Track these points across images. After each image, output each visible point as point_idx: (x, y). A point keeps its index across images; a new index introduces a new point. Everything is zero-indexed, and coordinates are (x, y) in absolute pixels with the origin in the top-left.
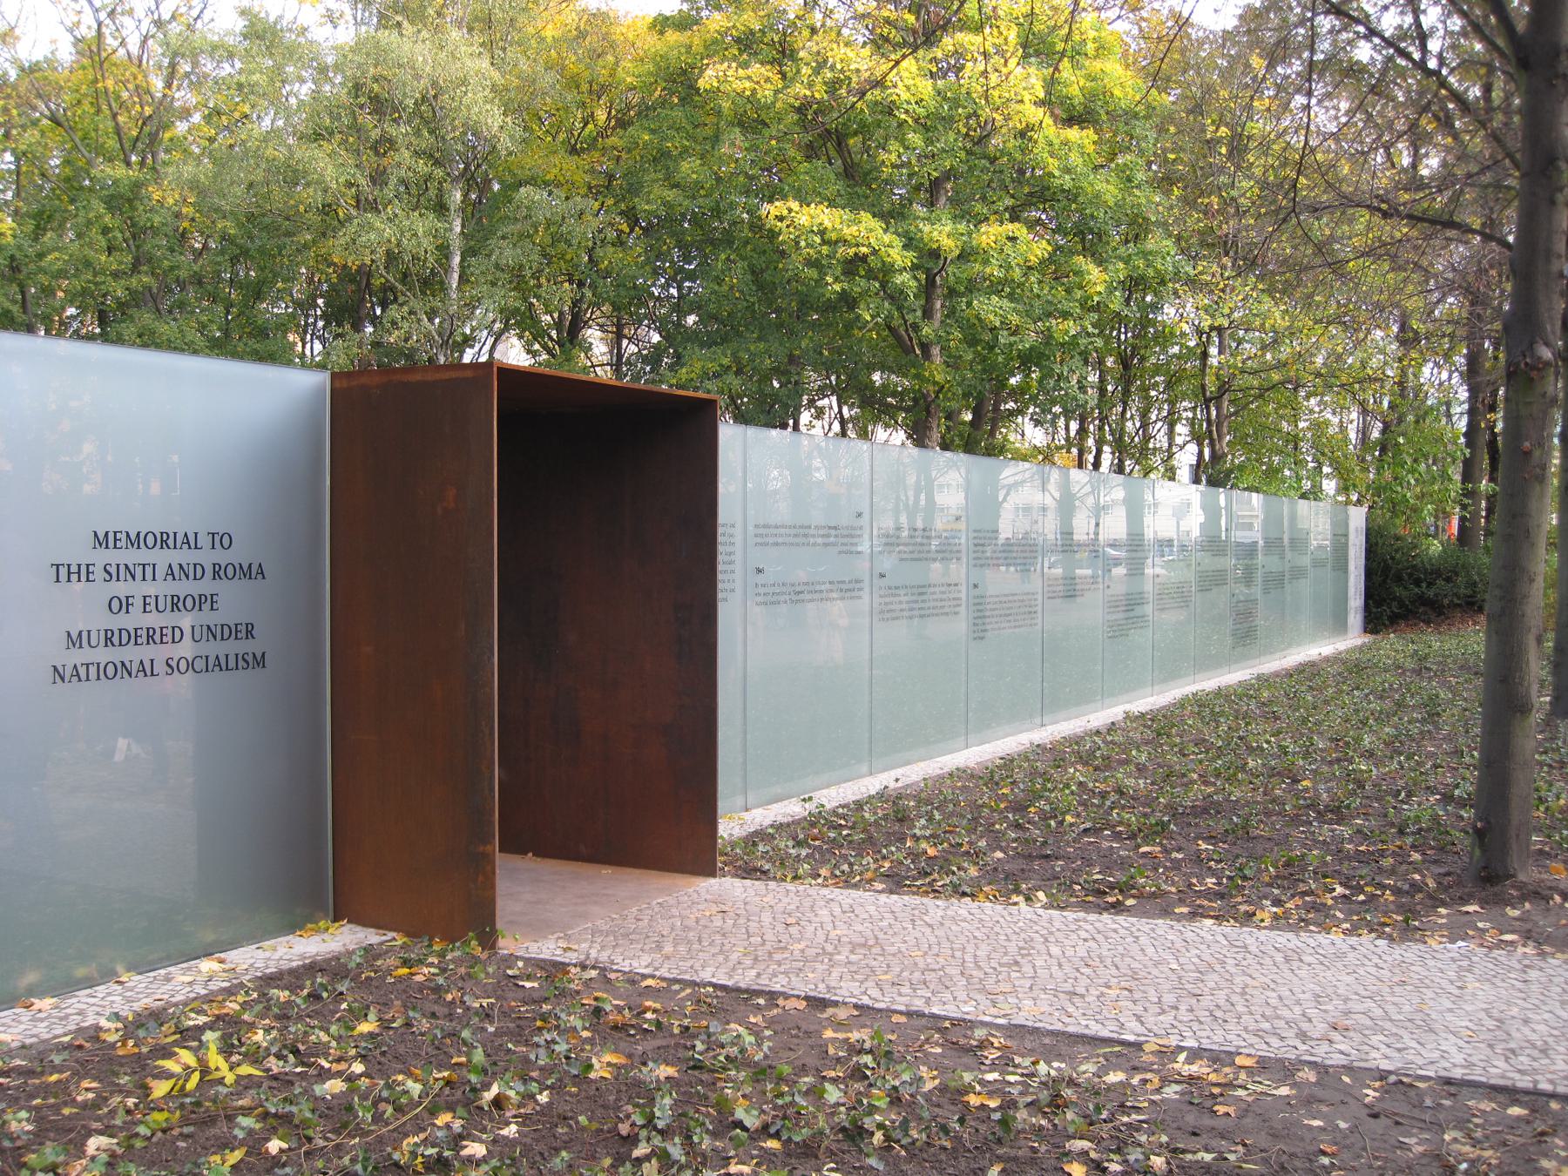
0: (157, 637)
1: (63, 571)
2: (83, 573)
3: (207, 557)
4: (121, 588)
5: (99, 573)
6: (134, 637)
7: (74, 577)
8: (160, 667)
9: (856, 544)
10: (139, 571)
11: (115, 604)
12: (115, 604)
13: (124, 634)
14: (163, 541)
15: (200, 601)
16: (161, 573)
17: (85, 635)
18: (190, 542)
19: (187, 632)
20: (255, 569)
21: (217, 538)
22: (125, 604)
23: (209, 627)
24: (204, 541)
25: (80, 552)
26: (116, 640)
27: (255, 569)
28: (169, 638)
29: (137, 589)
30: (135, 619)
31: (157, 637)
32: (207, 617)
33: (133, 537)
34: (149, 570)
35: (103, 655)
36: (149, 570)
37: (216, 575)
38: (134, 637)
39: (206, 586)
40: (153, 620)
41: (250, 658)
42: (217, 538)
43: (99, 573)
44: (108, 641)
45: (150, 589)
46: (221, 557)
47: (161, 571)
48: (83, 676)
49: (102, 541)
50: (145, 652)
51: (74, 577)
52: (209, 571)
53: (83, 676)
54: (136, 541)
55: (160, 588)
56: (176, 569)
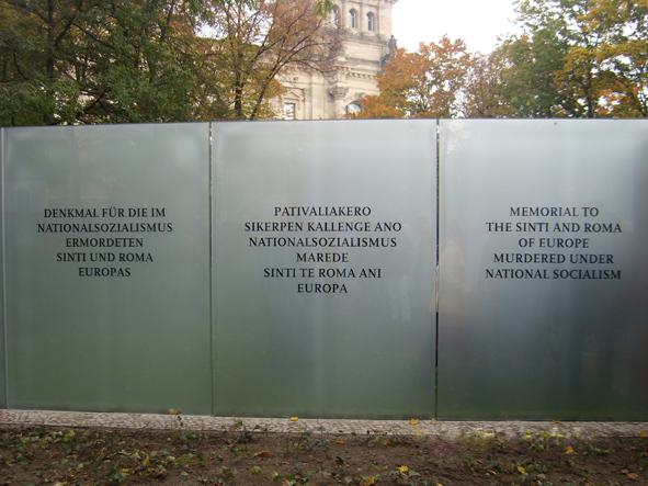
0: (548, 259)
1: (493, 226)
3: (581, 220)
4: (527, 235)
5: (514, 227)
7: (499, 229)
8: (550, 274)
10: (538, 227)
11: (523, 243)
12: (523, 243)
13: (528, 257)
15: (576, 243)
16: (551, 227)
17: (505, 257)
18: (571, 212)
20: (614, 226)
21: (588, 211)
22: (530, 242)
23: (582, 256)
24: (580, 212)
25: (506, 218)
26: (523, 259)
27: (614, 226)
28: (556, 260)
29: (536, 235)
30: (535, 249)
31: (548, 259)
32: (580, 250)
33: (534, 210)
34: (544, 227)
35: (515, 266)
36: (544, 227)
37: (587, 228)
39: (581, 234)
40: (547, 251)
41: (610, 273)
42: (588, 211)
43: (514, 227)
45: (544, 234)
46: (592, 221)
47: (551, 227)
48: (503, 275)
50: (541, 266)
51: (499, 229)
52: (583, 228)
53: (503, 275)
54: (537, 212)
55: (552, 235)
56: (561, 226)
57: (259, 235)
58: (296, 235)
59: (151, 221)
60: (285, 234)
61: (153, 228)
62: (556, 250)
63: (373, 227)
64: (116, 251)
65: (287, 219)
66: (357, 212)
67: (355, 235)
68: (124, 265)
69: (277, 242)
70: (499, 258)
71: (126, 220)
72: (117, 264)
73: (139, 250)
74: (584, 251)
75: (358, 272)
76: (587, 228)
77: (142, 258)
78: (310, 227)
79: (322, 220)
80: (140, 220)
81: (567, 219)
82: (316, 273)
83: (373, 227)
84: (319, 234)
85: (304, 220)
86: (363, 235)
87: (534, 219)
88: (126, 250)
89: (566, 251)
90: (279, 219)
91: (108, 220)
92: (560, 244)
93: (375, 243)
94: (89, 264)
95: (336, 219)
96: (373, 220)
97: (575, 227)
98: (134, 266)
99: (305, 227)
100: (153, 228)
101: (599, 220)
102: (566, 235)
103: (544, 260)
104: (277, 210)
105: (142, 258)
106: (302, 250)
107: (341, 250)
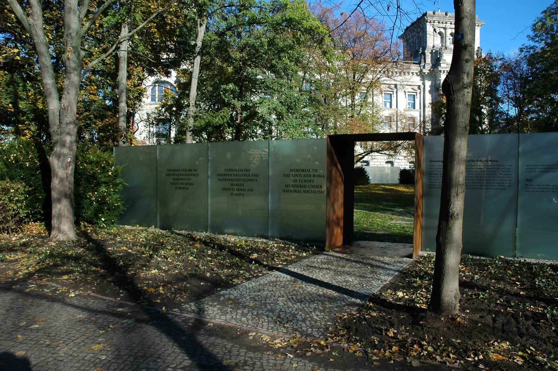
2: (288, 176)
3: (312, 174)
6: (297, 186)
8: (302, 191)
9: (526, 169)
14: (303, 170)
15: (310, 181)
16: (303, 176)
19: (308, 186)
22: (296, 181)
24: (311, 171)
29: (298, 178)
30: (298, 183)
35: (292, 189)
37: (314, 176)
38: (297, 186)
39: (312, 178)
40: (301, 184)
43: (291, 176)
44: (293, 186)
47: (303, 176)
49: (291, 170)
50: (300, 189)
52: (312, 176)
54: (298, 171)
57: (221, 177)
58: (230, 178)
59: (193, 173)
60: (228, 177)
61: (194, 175)
62: (304, 184)
63: (251, 175)
64: (184, 182)
65: (228, 173)
66: (247, 171)
67: (246, 178)
68: (187, 186)
69: (225, 180)
70: (287, 186)
71: (187, 173)
72: (185, 186)
73: (190, 182)
74: (313, 184)
75: (247, 190)
76: (314, 176)
77: (191, 184)
78: (234, 175)
79: (237, 173)
80: (191, 173)
81: (308, 173)
82: (236, 190)
83: (251, 175)
84: (236, 177)
85: (232, 173)
86: (248, 178)
87: (297, 173)
88: (187, 182)
89: (306, 184)
90: (227, 173)
91: (183, 173)
92: (305, 181)
93: (251, 180)
94: (178, 186)
95: (241, 173)
96: (251, 173)
97: (310, 176)
98: (189, 186)
99: (233, 175)
100: (194, 175)
101: (318, 173)
102: (306, 179)
103: (300, 187)
104: (225, 170)
105: (191, 184)
106: (232, 182)
107: (242, 183)
